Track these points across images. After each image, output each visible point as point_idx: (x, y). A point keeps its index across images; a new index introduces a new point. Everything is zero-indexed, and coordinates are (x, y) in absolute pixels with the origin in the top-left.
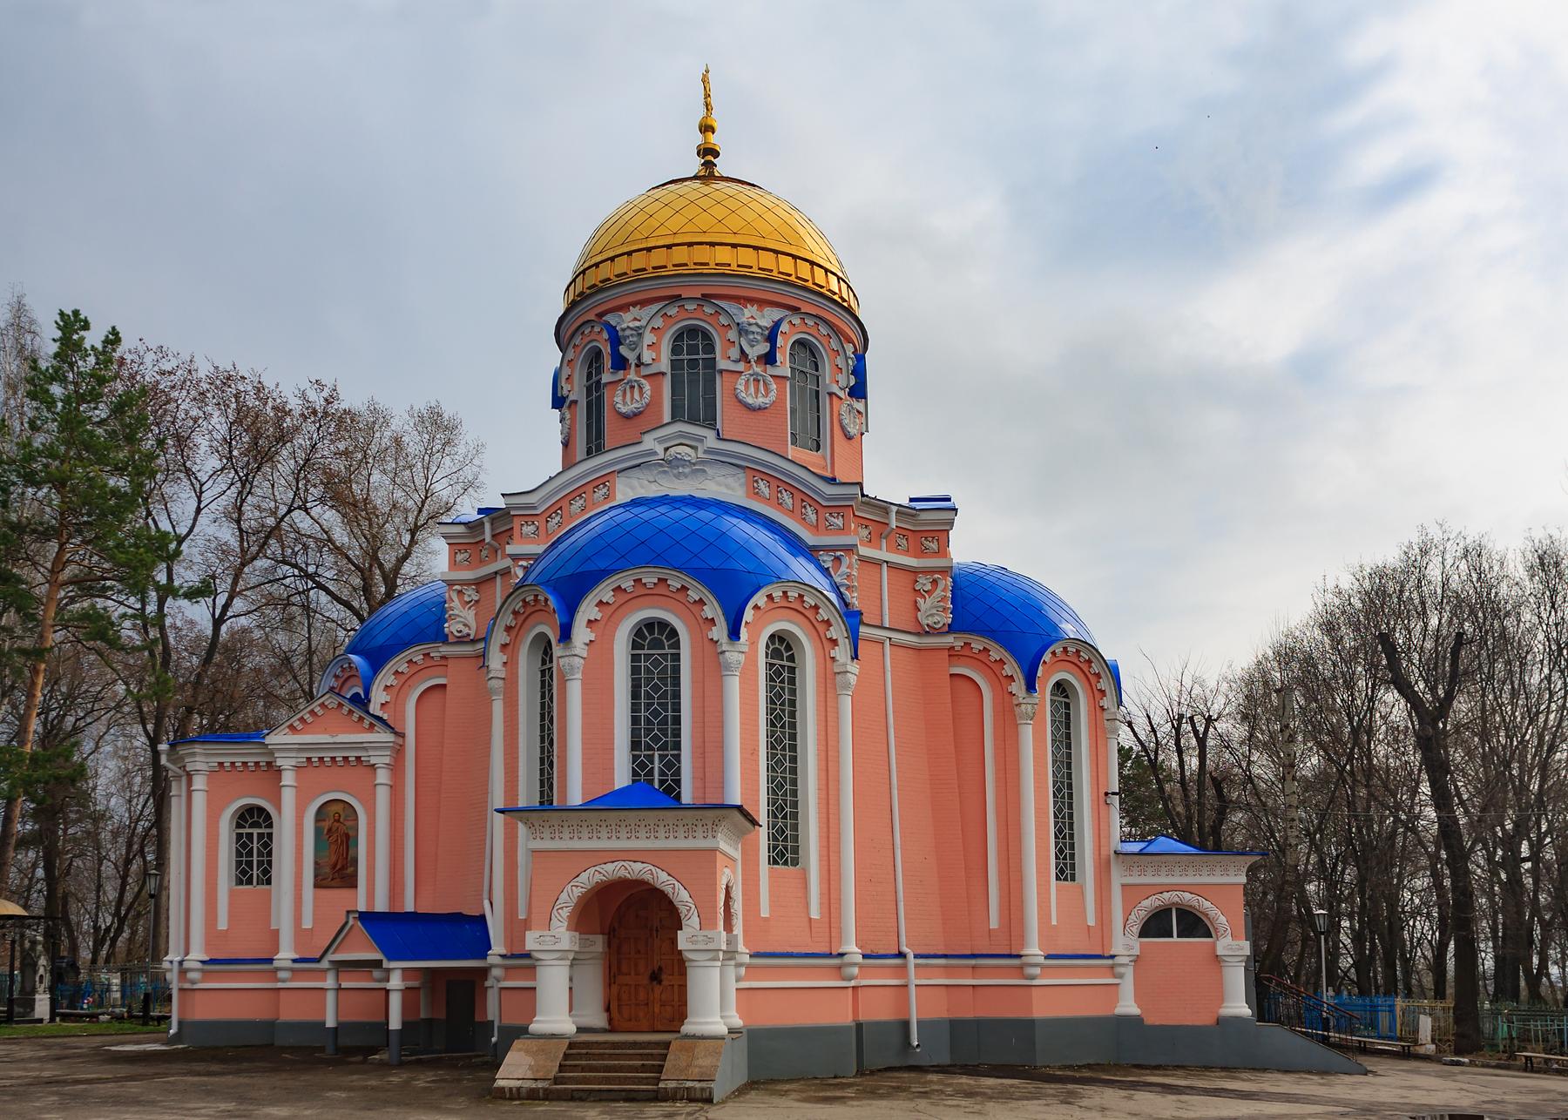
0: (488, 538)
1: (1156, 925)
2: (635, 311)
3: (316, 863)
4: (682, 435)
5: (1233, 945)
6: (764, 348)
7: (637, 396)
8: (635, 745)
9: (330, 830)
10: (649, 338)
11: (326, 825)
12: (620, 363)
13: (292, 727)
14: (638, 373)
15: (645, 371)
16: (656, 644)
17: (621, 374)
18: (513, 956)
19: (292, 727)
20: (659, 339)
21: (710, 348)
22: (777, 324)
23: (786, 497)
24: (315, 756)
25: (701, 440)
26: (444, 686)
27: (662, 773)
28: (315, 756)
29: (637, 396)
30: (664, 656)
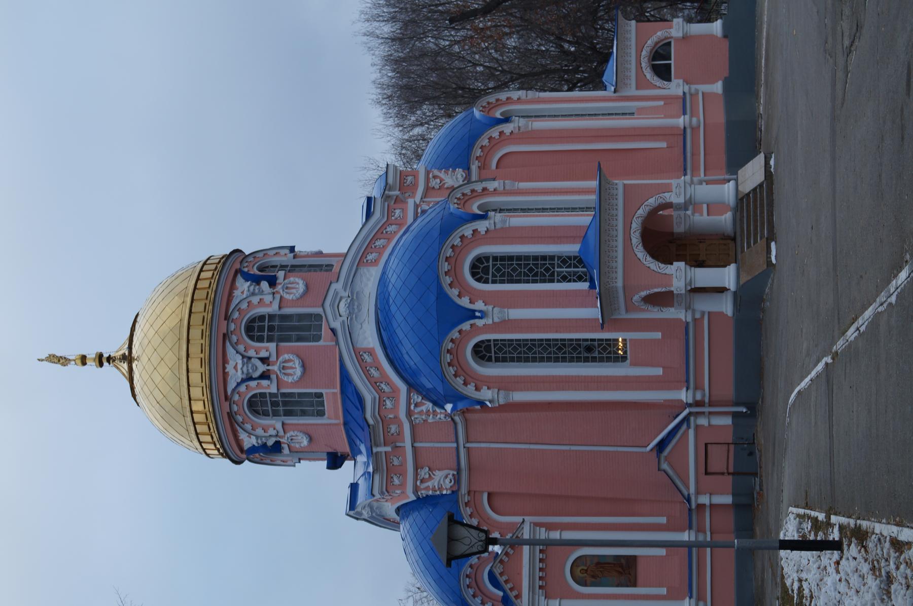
0: (388, 449)
1: (663, 73)
2: (230, 368)
3: (618, 586)
4: (332, 305)
5: (677, 28)
6: (265, 285)
7: (290, 364)
8: (552, 281)
9: (593, 577)
10: (251, 353)
11: (589, 580)
12: (265, 376)
13: (517, 597)
14: (274, 364)
15: (273, 358)
16: (486, 270)
17: (273, 377)
18: (688, 381)
19: (517, 597)
20: (253, 347)
21: (262, 318)
22: (248, 277)
23: (378, 243)
24: (538, 583)
25: (336, 293)
26: (489, 495)
27: (569, 266)
28: (538, 583)
29: (290, 364)
30: (494, 265)
